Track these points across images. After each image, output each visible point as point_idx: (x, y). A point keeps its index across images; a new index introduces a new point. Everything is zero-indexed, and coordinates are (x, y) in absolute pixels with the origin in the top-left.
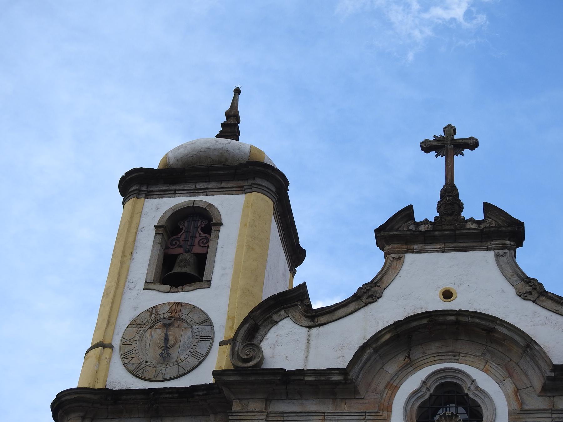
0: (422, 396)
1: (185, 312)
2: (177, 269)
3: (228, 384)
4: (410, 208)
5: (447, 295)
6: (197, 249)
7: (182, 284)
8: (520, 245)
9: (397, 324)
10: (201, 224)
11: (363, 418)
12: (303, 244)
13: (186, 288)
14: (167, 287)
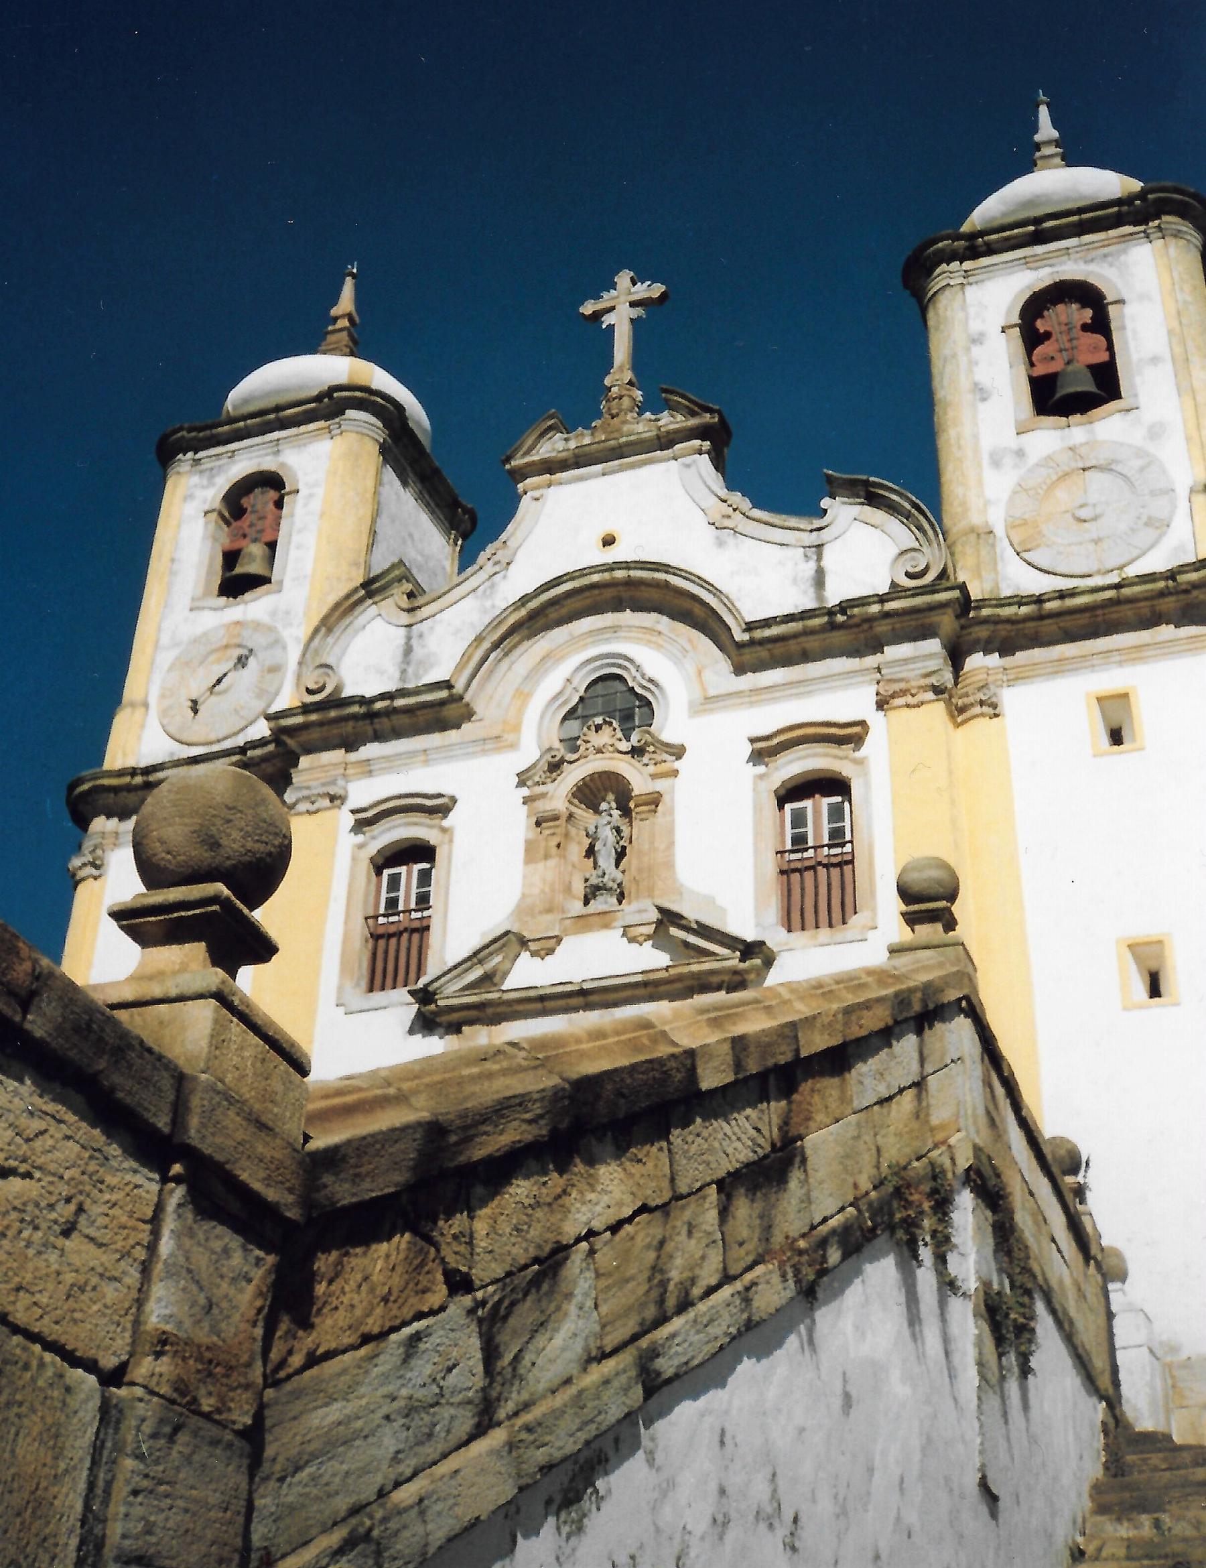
0: (565, 702)
2: (239, 570)
5: (608, 541)
9: (525, 600)
10: (272, 495)
11: (479, 749)
13: (248, 596)
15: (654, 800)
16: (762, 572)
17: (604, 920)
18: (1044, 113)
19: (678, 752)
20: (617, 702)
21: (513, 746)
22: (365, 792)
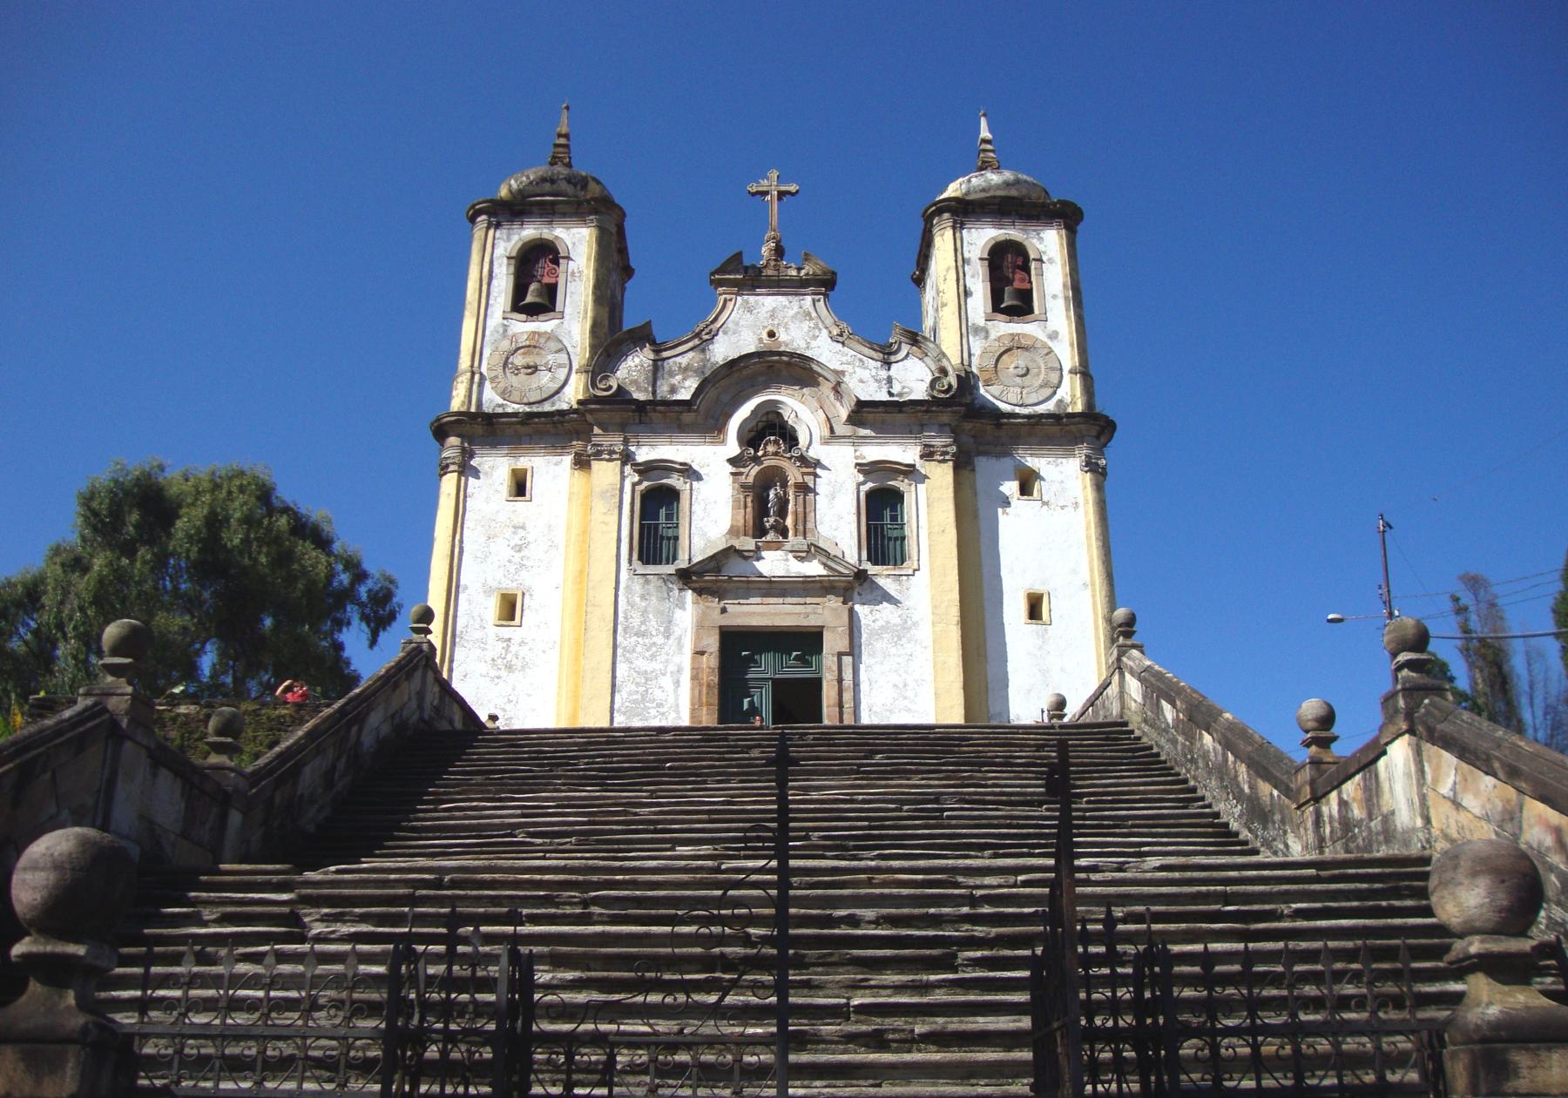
1: (542, 340)
2: (529, 299)
3: (591, 411)
4: (740, 254)
6: (546, 280)
7: (537, 314)
8: (832, 289)
12: (633, 264)
13: (541, 317)
14: (523, 317)
15: (805, 489)
16: (866, 381)
17: (777, 546)
18: (983, 122)
19: (818, 464)
20: (771, 429)
21: (723, 442)
22: (644, 454)
